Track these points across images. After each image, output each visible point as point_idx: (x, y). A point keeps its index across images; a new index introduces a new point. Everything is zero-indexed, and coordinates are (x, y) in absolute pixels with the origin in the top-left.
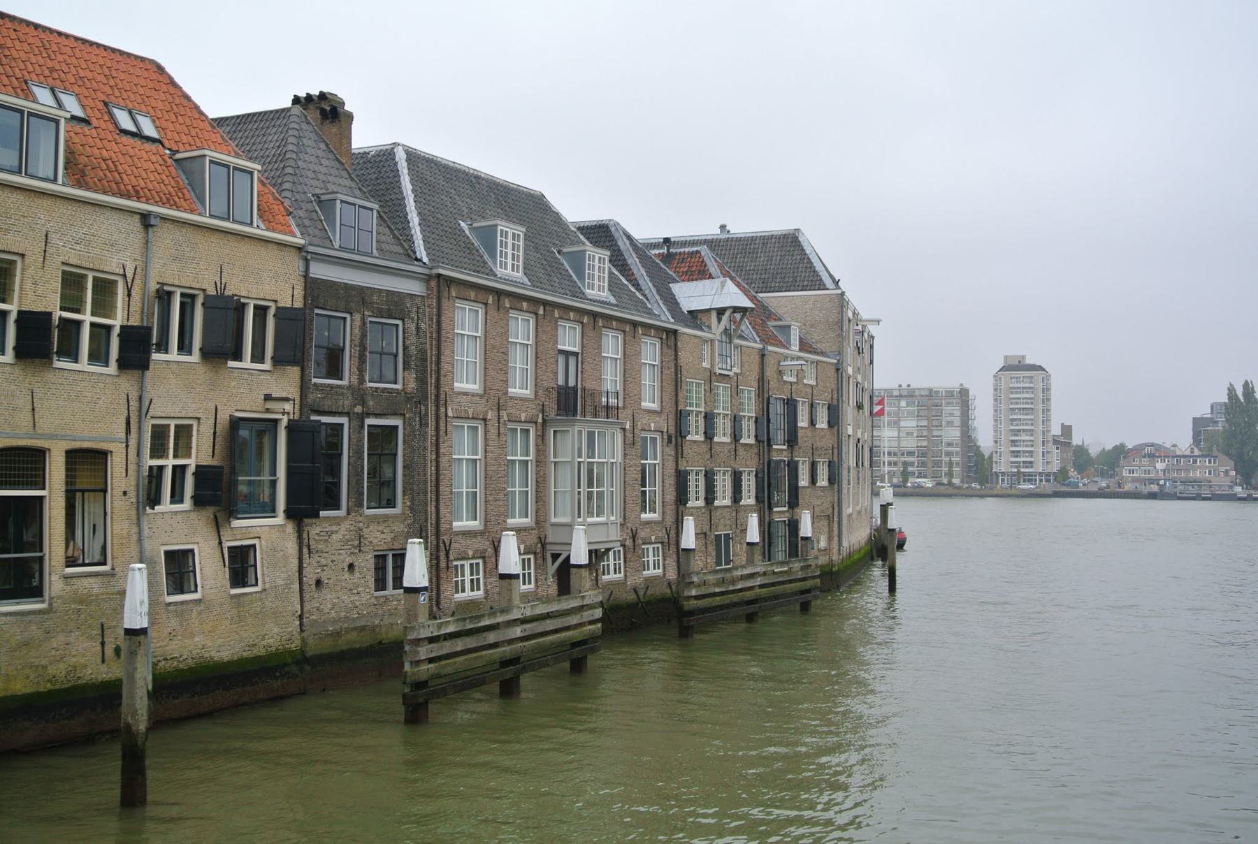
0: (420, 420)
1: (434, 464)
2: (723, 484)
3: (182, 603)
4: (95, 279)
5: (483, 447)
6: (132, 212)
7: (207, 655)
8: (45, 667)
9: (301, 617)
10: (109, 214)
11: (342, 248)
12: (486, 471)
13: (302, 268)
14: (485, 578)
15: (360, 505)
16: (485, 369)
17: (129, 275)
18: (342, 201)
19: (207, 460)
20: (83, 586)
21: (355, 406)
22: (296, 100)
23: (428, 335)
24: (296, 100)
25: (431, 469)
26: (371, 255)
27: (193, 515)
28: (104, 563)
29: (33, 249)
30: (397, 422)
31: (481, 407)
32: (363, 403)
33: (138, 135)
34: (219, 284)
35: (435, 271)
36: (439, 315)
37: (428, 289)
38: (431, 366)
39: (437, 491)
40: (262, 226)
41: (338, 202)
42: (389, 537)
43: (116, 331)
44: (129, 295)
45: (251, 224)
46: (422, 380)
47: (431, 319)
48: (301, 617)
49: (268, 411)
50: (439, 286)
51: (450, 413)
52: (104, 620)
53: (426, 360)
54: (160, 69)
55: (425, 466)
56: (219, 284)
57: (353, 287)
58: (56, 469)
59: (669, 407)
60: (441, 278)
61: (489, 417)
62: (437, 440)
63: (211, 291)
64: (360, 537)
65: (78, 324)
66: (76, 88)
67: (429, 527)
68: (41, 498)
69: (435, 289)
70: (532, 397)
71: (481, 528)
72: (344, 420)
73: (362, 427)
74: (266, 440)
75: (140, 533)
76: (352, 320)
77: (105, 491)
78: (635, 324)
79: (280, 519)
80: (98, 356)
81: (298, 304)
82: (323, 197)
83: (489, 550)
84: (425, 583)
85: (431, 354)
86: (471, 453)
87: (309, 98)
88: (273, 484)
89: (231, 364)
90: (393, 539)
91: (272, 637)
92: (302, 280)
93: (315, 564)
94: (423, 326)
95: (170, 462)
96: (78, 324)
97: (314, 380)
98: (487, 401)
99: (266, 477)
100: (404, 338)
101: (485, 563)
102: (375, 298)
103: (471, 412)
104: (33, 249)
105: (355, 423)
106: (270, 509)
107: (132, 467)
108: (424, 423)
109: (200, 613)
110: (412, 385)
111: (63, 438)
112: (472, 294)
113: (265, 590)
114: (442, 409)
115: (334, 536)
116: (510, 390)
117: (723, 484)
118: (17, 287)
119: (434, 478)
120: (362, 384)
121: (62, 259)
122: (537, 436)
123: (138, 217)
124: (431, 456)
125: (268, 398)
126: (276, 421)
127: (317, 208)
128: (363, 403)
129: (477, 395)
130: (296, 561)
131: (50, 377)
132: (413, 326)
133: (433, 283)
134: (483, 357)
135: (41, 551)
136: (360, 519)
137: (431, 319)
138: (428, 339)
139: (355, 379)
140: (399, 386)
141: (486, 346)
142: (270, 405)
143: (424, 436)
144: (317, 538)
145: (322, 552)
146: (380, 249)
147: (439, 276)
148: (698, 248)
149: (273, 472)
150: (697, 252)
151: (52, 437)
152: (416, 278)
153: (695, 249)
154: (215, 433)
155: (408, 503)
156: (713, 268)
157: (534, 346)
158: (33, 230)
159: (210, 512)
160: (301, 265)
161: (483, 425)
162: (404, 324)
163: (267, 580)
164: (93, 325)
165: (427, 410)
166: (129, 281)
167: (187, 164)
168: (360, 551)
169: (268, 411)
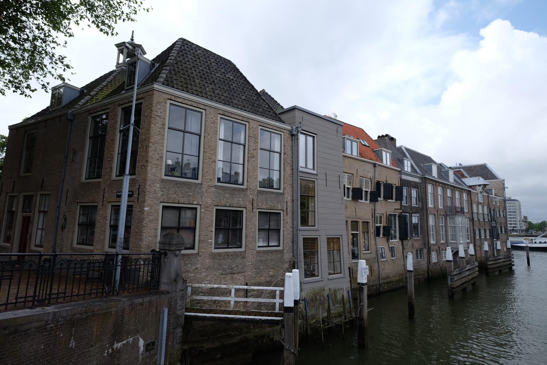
2: (482, 232)
10: (368, 164)
16: (434, 201)
19: (385, 225)
22: (379, 137)
24: (379, 137)
28: (369, 250)
33: (365, 145)
35: (424, 176)
42: (418, 245)
43: (369, 192)
46: (422, 204)
49: (395, 212)
50: (425, 180)
54: (363, 130)
59: (470, 212)
63: (385, 183)
68: (357, 234)
70: (443, 208)
72: (408, 214)
78: (462, 189)
79: (398, 240)
81: (399, 185)
82: (400, 159)
84: (452, 260)
87: (383, 136)
89: (359, 201)
90: (419, 246)
103: (432, 212)
105: (410, 215)
109: (387, 264)
110: (421, 206)
113: (397, 258)
115: (408, 245)
117: (482, 232)
122: (445, 219)
123: (373, 165)
131: (358, 204)
133: (424, 180)
142: (396, 211)
147: (425, 177)
148: (460, 169)
150: (460, 170)
153: (459, 170)
156: (466, 175)
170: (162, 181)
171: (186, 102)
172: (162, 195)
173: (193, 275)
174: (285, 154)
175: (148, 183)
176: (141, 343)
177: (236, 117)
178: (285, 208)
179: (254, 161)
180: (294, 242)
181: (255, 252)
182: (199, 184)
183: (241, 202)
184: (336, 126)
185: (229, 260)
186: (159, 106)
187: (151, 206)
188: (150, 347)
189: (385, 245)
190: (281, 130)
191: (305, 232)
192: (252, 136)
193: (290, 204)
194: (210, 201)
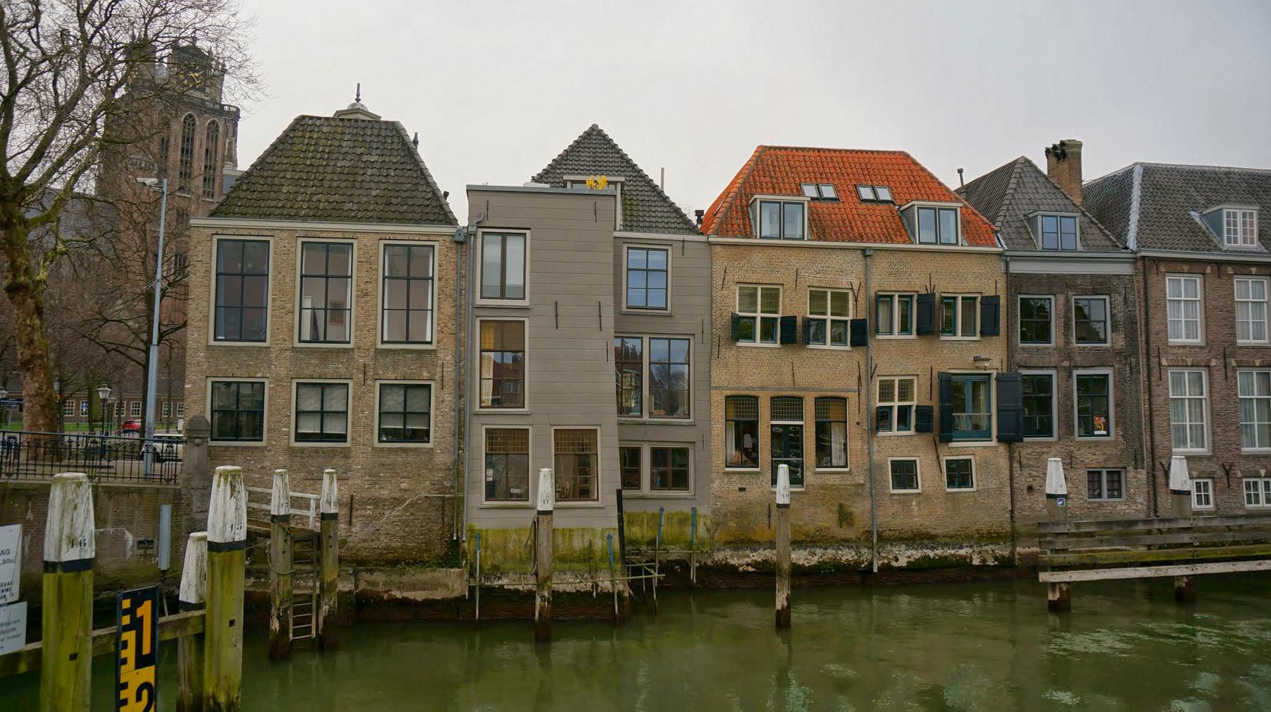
0: (1131, 369)
1: (1147, 402)
3: (904, 495)
4: (832, 293)
5: (1208, 390)
6: (855, 249)
7: (925, 530)
8: (801, 526)
9: (1012, 511)
10: (839, 253)
11: (1044, 250)
12: (1212, 408)
13: (1003, 267)
14: (1215, 494)
15: (1072, 433)
16: (1207, 326)
17: (856, 288)
18: (1043, 216)
20: (831, 480)
21: (1062, 361)
23: (1137, 304)
25: (1144, 407)
26: (1075, 251)
27: (915, 439)
28: (846, 467)
29: (789, 280)
30: (1108, 371)
31: (1203, 357)
32: (1070, 358)
33: (877, 201)
34: (928, 287)
35: (1139, 255)
36: (1145, 288)
37: (1136, 269)
38: (1140, 327)
39: (1151, 423)
40: (965, 243)
41: (1039, 217)
42: (1101, 458)
44: (856, 301)
45: (957, 244)
46: (1131, 338)
47: (1139, 292)
48: (1012, 511)
49: (977, 368)
50: (1144, 266)
51: (1164, 362)
52: (843, 502)
53: (1136, 323)
54: (907, 156)
55: (1139, 404)
56: (928, 287)
57: (1056, 276)
58: (809, 408)
60: (1146, 259)
61: (1213, 363)
62: (1149, 380)
63: (923, 292)
64: (1071, 457)
65: (825, 321)
66: (837, 182)
67: (1145, 452)
68: (802, 426)
69: (1141, 268)
71: (1210, 454)
73: (1070, 376)
74: (982, 389)
75: (869, 449)
76: (1056, 300)
77: (846, 422)
79: (994, 443)
80: (837, 339)
82: (1030, 216)
83: (1219, 472)
85: (1139, 314)
86: (1192, 393)
88: (990, 417)
91: (984, 524)
92: (1005, 276)
93: (1027, 475)
94: (1131, 297)
95: (896, 404)
96: (825, 321)
97: (1021, 345)
98: (1209, 352)
99: (983, 414)
100: (1111, 308)
101: (1215, 483)
102: (1079, 282)
104: (789, 280)
105: (1063, 374)
106: (987, 436)
107: (863, 407)
108: (1134, 370)
111: (813, 390)
112: (1186, 268)
113: (978, 491)
114: (1154, 361)
116: (1238, 341)
118: (781, 303)
119: (1147, 413)
120: (1068, 345)
121: (808, 284)
123: (859, 252)
124: (1144, 397)
125: (977, 359)
126: (989, 374)
127: (1027, 224)
128: (1070, 358)
129: (1201, 347)
130: (1007, 472)
131: (804, 354)
132: (1120, 299)
133: (1140, 264)
134: (1203, 316)
135: (802, 457)
136: (1071, 444)
137: (1139, 292)
138: (1138, 309)
139: (1061, 344)
140: (1108, 345)
141: (1205, 307)
142: (978, 364)
143: (1136, 382)
144: (1028, 456)
145: (1033, 467)
146: (1086, 245)
147: (1144, 257)
149: (989, 410)
151: (805, 389)
152: (1128, 262)
154: (931, 384)
155: (1121, 433)
157: (1202, 301)
158: (788, 269)
159: (928, 437)
160: (1003, 265)
161: (1207, 371)
162: (1111, 298)
163: (980, 484)
164: (762, 318)
165: (1138, 364)
166: (856, 291)
167: (906, 213)
168: (1071, 467)
169: (977, 368)
170: (208, 347)
171: (240, 232)
172: (209, 368)
173: (258, 476)
174: (440, 279)
175: (189, 353)
176: (130, 537)
177: (330, 235)
178: (438, 377)
179: (367, 302)
180: (460, 432)
181: (370, 449)
182: (266, 348)
183: (343, 371)
184: (591, 201)
185: (320, 460)
186: (200, 248)
187: (194, 383)
188: (146, 544)
189: (920, 454)
190: (434, 238)
191: (506, 420)
192: (364, 260)
193: (450, 369)
194: (283, 372)
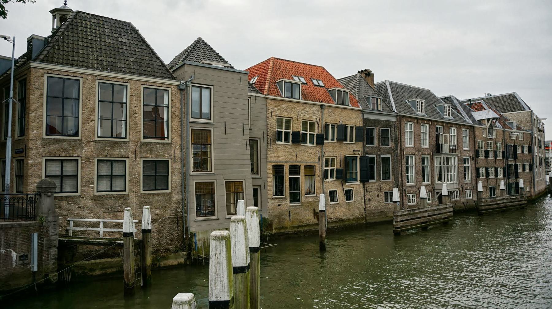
2: (492, 172)
3: (334, 204)
7: (340, 218)
8: (301, 219)
9: (365, 209)
14: (416, 199)
15: (380, 179)
17: (318, 121)
18: (372, 97)
19: (339, 168)
22: (359, 72)
24: (359, 72)
25: (400, 169)
28: (314, 194)
29: (295, 116)
31: (414, 151)
32: (380, 151)
33: (319, 86)
36: (400, 126)
38: (399, 141)
39: (402, 175)
40: (351, 106)
42: (388, 187)
43: (316, 135)
44: (318, 126)
45: (348, 106)
46: (396, 144)
48: (365, 209)
49: (354, 154)
50: (400, 118)
51: (405, 153)
54: (324, 69)
59: (473, 149)
62: (401, 160)
63: (339, 124)
65: (306, 134)
66: (304, 76)
68: (299, 178)
70: (429, 148)
71: (415, 185)
72: (375, 156)
73: (380, 158)
74: (354, 162)
75: (323, 186)
76: (376, 129)
77: (314, 176)
78: (460, 125)
79: (359, 183)
80: (311, 142)
81: (361, 126)
82: (367, 97)
84: (399, 200)
85: (398, 137)
87: (362, 71)
88: (357, 173)
89: (344, 142)
90: (390, 188)
95: (330, 168)
97: (366, 146)
99: (354, 172)
101: (416, 195)
102: (382, 123)
103: (410, 152)
104: (295, 116)
105: (378, 157)
106: (356, 180)
108: (397, 156)
109: (338, 207)
110: (393, 146)
114: (402, 152)
115: (373, 187)
117: (492, 172)
119: (401, 171)
121: (302, 118)
122: (431, 159)
123: (319, 107)
124: (400, 165)
125: (354, 151)
128: (380, 151)
129: (413, 148)
130: (363, 194)
131: (300, 147)
133: (398, 117)
140: (390, 146)
141: (414, 134)
142: (355, 153)
143: (397, 160)
147: (400, 115)
148: (480, 101)
149: (356, 170)
150: (480, 102)
153: (479, 102)
156: (485, 107)
163: (356, 198)
164: (310, 134)
165: (398, 152)
167: (331, 92)
169: (354, 154)
170: (43, 139)
171: (63, 73)
172: (44, 151)
173: (76, 212)
174: (172, 107)
175: (31, 142)
176: (14, 255)
177: (115, 80)
178: (172, 157)
179: (135, 117)
180: (184, 185)
181: (139, 194)
182: (79, 140)
183: (123, 153)
184: (240, 75)
185: (112, 201)
186: (36, 80)
187: (35, 160)
188: (23, 258)
189: (338, 188)
190: (168, 86)
191: (203, 177)
192: (134, 95)
193: (178, 153)
194: (90, 154)
